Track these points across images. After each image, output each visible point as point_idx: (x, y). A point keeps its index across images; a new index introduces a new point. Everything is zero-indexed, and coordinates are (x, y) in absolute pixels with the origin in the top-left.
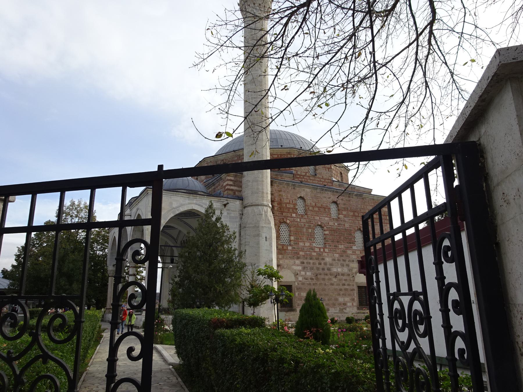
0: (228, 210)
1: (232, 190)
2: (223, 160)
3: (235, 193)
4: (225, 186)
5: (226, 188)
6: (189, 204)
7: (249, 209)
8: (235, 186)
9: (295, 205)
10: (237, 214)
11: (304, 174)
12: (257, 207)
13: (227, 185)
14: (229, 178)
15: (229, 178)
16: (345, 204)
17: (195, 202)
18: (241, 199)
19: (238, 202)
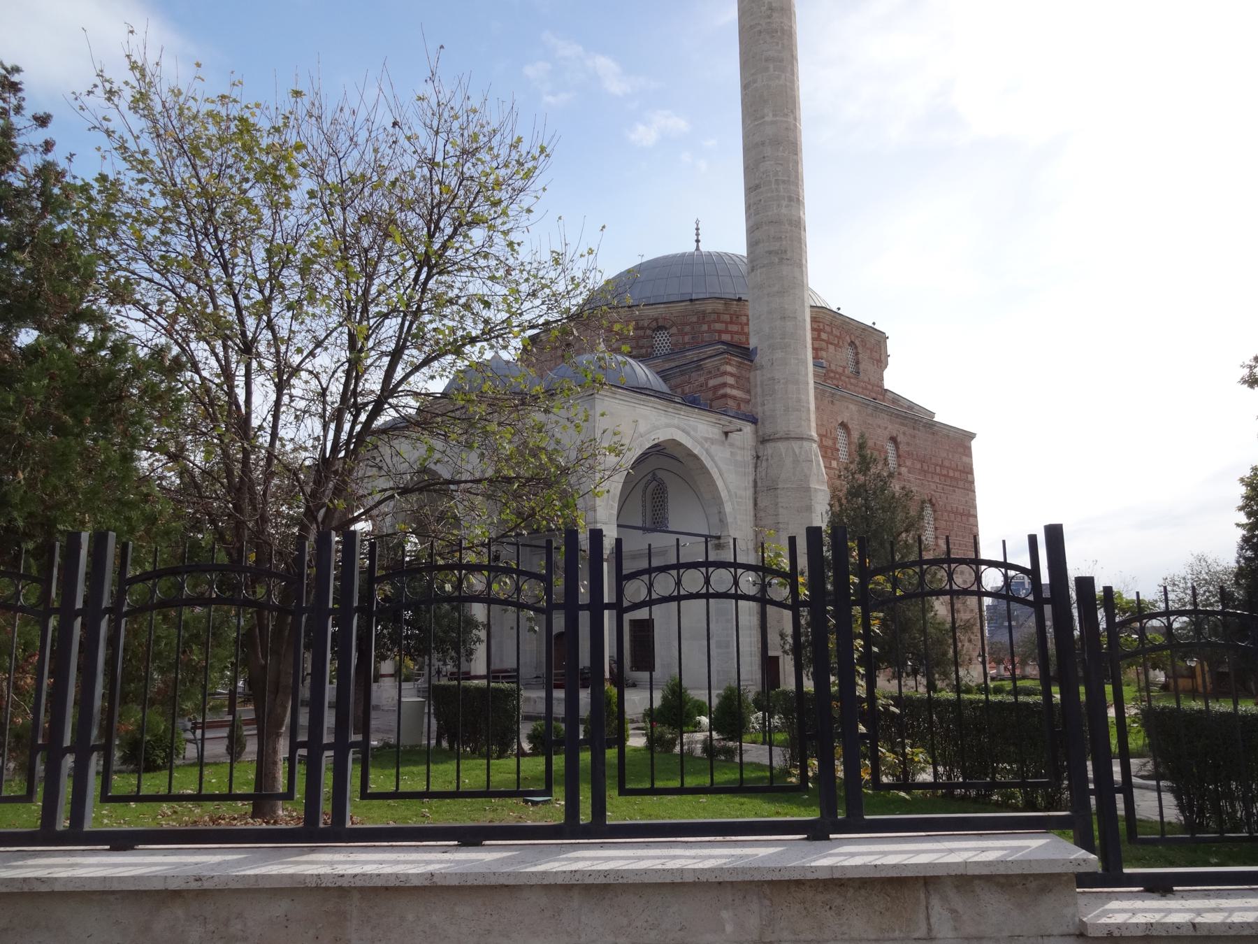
0: (732, 445)
1: (734, 398)
2: (656, 320)
3: (739, 405)
4: (716, 388)
5: (722, 392)
6: (668, 426)
7: (781, 446)
8: (738, 388)
9: (835, 440)
10: (748, 456)
11: (840, 370)
12: (799, 442)
13: (724, 385)
14: (729, 368)
15: (729, 368)
16: (908, 444)
17: (676, 421)
18: (754, 421)
19: (748, 428)
